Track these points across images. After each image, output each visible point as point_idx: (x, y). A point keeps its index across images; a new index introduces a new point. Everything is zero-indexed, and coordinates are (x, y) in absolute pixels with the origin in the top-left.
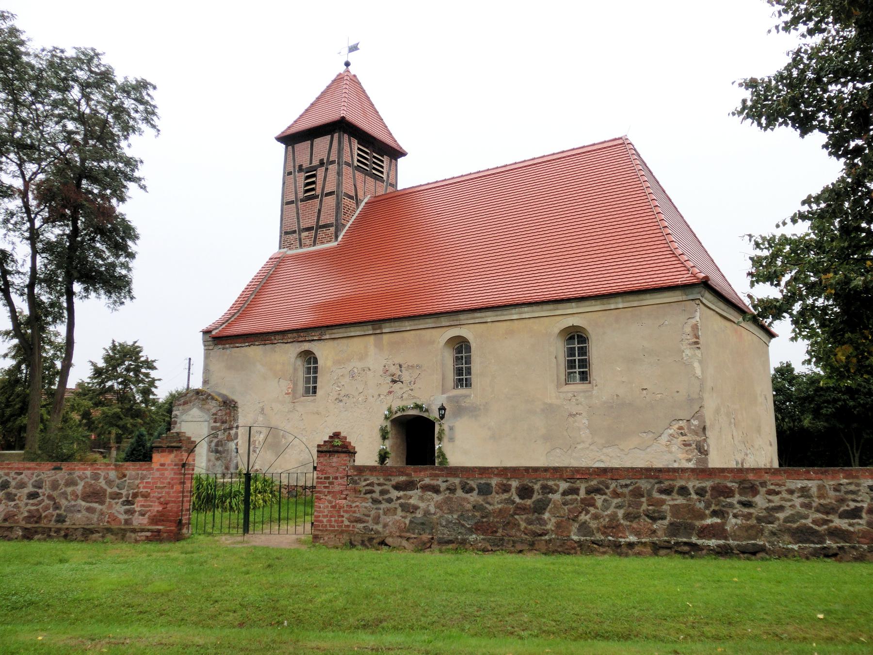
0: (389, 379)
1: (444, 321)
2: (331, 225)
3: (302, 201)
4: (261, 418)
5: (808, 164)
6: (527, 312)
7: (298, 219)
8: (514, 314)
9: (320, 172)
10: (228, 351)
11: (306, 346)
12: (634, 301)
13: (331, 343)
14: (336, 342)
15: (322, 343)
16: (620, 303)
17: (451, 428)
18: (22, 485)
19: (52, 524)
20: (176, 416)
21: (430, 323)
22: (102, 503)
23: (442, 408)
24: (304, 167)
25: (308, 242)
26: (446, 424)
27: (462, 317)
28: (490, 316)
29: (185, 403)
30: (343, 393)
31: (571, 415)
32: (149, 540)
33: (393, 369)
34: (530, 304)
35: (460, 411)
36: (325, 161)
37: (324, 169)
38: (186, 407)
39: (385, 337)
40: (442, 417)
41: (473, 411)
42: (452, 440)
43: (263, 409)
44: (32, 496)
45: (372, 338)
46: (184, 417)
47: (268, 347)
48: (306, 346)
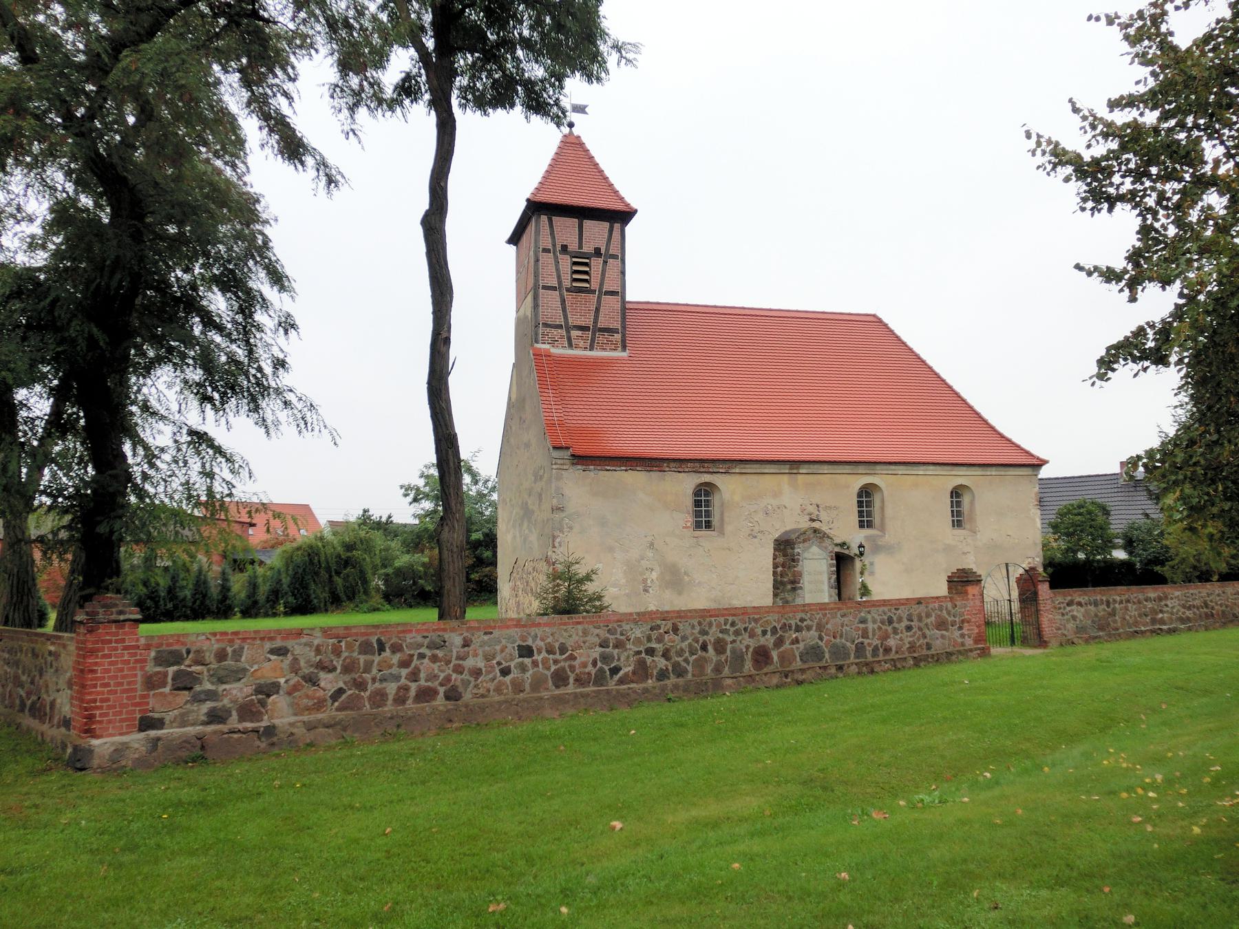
0: (808, 517)
1: (861, 469)
2: (615, 331)
3: (568, 290)
4: (650, 554)
5: (1154, 406)
6: (931, 470)
7: (564, 310)
8: (921, 470)
9: (596, 264)
10: (592, 474)
11: (707, 478)
12: (1002, 471)
13: (737, 476)
14: (744, 477)
15: (728, 477)
16: (993, 471)
17: (872, 564)
18: (900, 620)
19: (925, 652)
20: (798, 554)
21: (847, 469)
22: (947, 630)
23: (861, 546)
24: (570, 248)
25: (581, 344)
26: (867, 559)
27: (878, 467)
28: (901, 470)
29: (804, 541)
30: (756, 529)
31: (964, 553)
32: (979, 656)
33: (812, 509)
34: (979, 465)
35: (877, 549)
36: (603, 251)
37: (601, 260)
38: (806, 544)
39: (800, 477)
40: (862, 554)
41: (889, 549)
42: (872, 573)
43: (652, 544)
44: (909, 628)
45: (785, 477)
46: (806, 555)
47: (654, 475)
48: (707, 478)
